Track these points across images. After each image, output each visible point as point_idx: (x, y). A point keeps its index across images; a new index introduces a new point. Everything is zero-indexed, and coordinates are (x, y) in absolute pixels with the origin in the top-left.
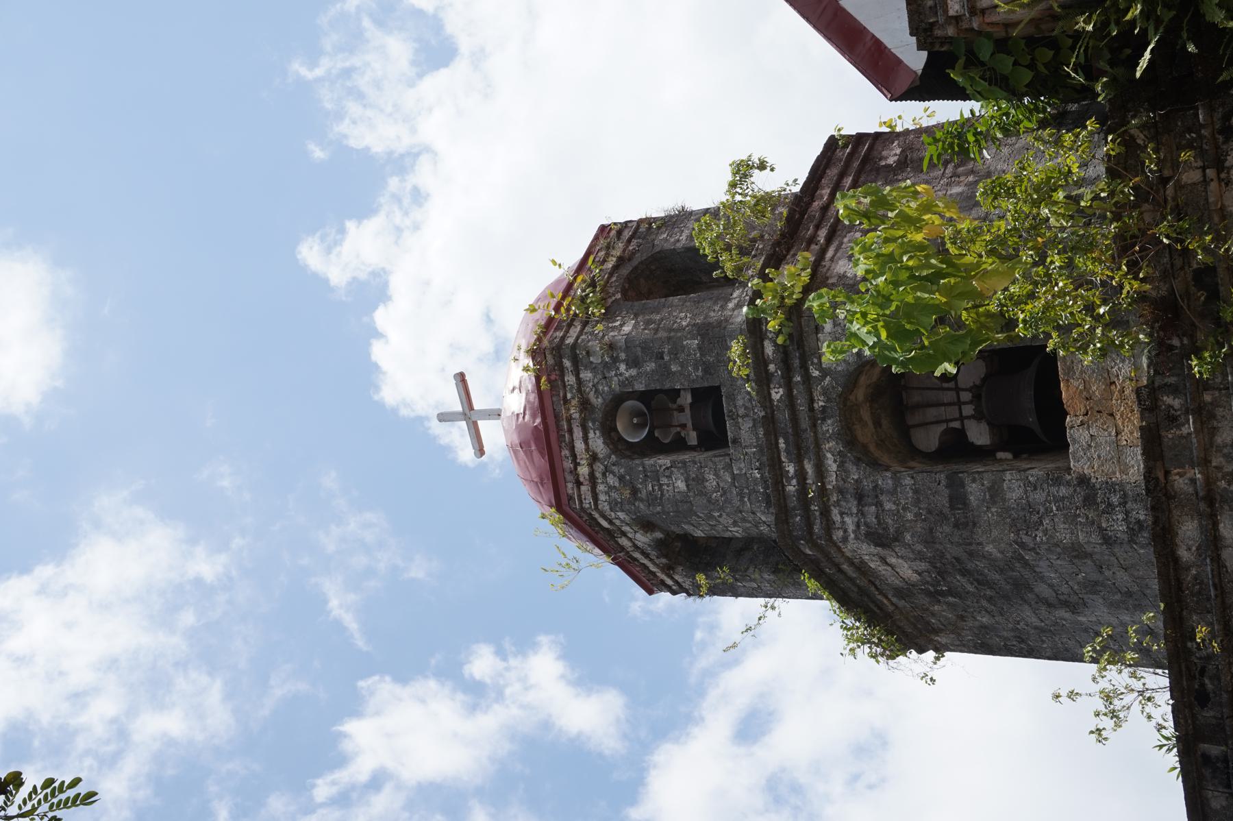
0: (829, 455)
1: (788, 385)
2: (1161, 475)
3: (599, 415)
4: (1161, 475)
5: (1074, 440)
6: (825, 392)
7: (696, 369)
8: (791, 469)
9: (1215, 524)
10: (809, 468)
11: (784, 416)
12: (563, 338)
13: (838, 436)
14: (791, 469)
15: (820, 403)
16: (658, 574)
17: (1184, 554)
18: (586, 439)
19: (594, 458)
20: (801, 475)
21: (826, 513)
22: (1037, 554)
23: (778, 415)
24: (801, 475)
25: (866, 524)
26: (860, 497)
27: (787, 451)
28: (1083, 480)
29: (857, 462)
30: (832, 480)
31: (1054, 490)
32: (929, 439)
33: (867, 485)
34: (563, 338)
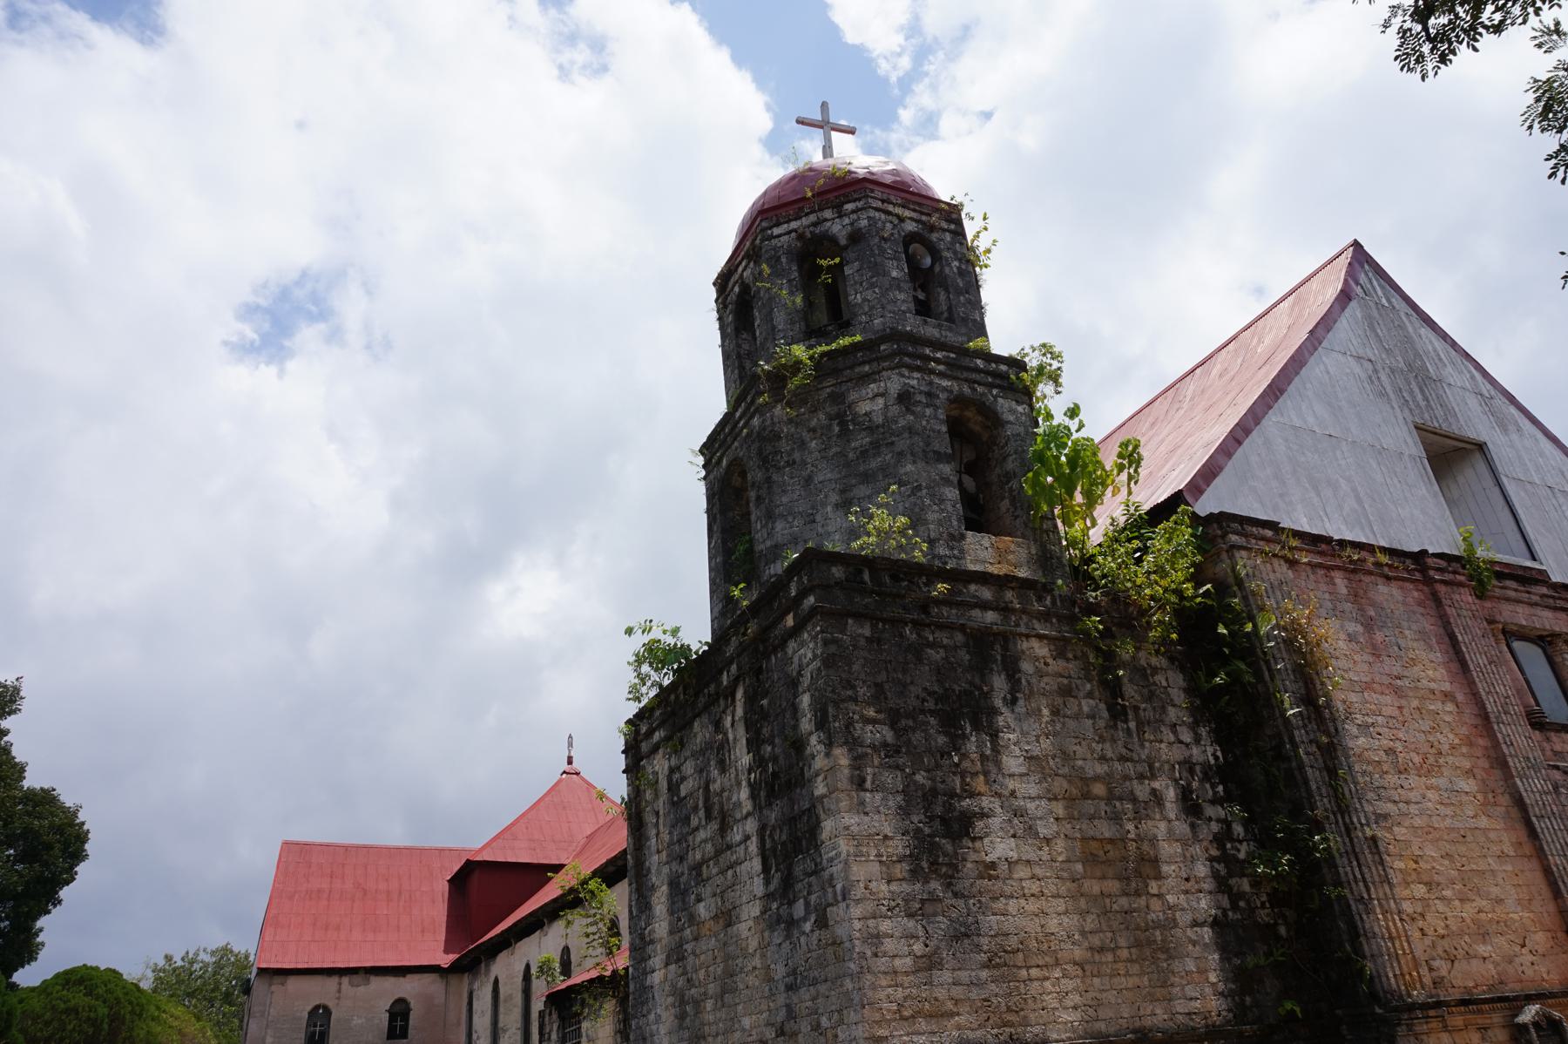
0: (950, 383)
2: (1013, 585)
3: (927, 235)
4: (1013, 585)
5: (983, 537)
6: (983, 394)
7: (963, 313)
8: (939, 355)
9: (992, 609)
11: (966, 362)
14: (939, 355)
15: (980, 389)
16: (786, 225)
17: (973, 587)
21: (918, 369)
22: (909, 496)
23: (968, 359)
25: (914, 393)
27: (948, 357)
31: (955, 517)
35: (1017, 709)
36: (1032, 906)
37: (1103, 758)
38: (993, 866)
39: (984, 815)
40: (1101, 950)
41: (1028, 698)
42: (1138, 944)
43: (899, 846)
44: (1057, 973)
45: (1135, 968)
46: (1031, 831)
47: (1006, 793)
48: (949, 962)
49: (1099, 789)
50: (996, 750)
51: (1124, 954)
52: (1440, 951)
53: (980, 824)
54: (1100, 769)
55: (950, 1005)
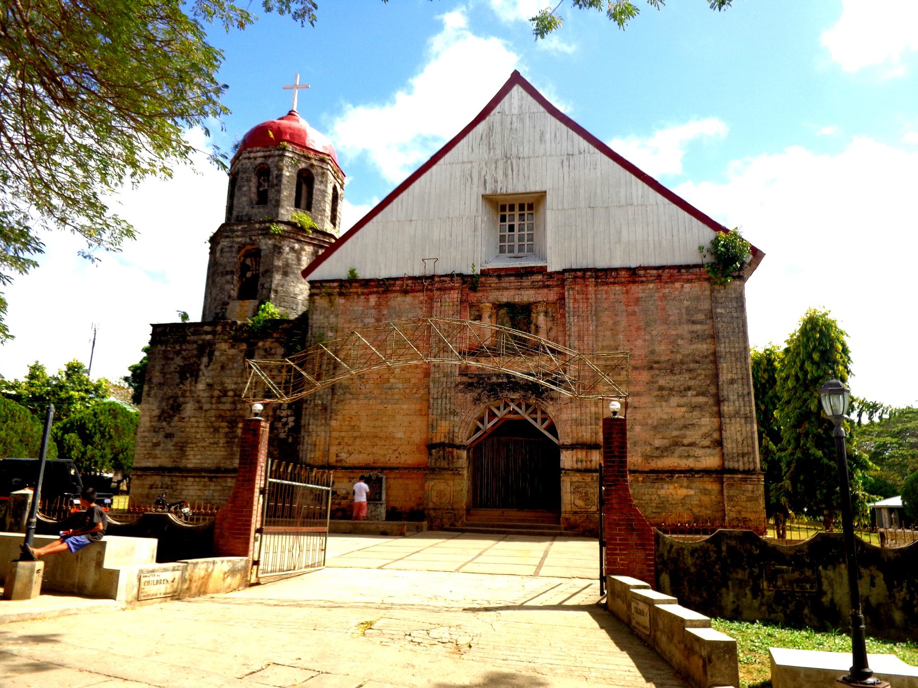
1: (259, 229)
10: (239, 233)
12: (288, 151)
13: (245, 242)
14: (239, 228)
18: (260, 157)
19: (255, 158)
20: (237, 231)
24: (237, 231)
26: (231, 247)
28: (228, 303)
29: (239, 247)
30: (236, 239)
32: (248, 262)
33: (234, 249)
34: (288, 151)
35: (209, 368)
36: (193, 430)
37: (236, 383)
38: (184, 418)
39: (186, 403)
40: (214, 443)
41: (214, 364)
42: (227, 442)
43: (157, 412)
44: (196, 449)
45: (223, 449)
46: (201, 408)
47: (196, 396)
48: (162, 445)
49: (231, 393)
50: (196, 383)
51: (221, 445)
52: (345, 450)
53: (184, 406)
54: (233, 387)
55: (159, 456)
